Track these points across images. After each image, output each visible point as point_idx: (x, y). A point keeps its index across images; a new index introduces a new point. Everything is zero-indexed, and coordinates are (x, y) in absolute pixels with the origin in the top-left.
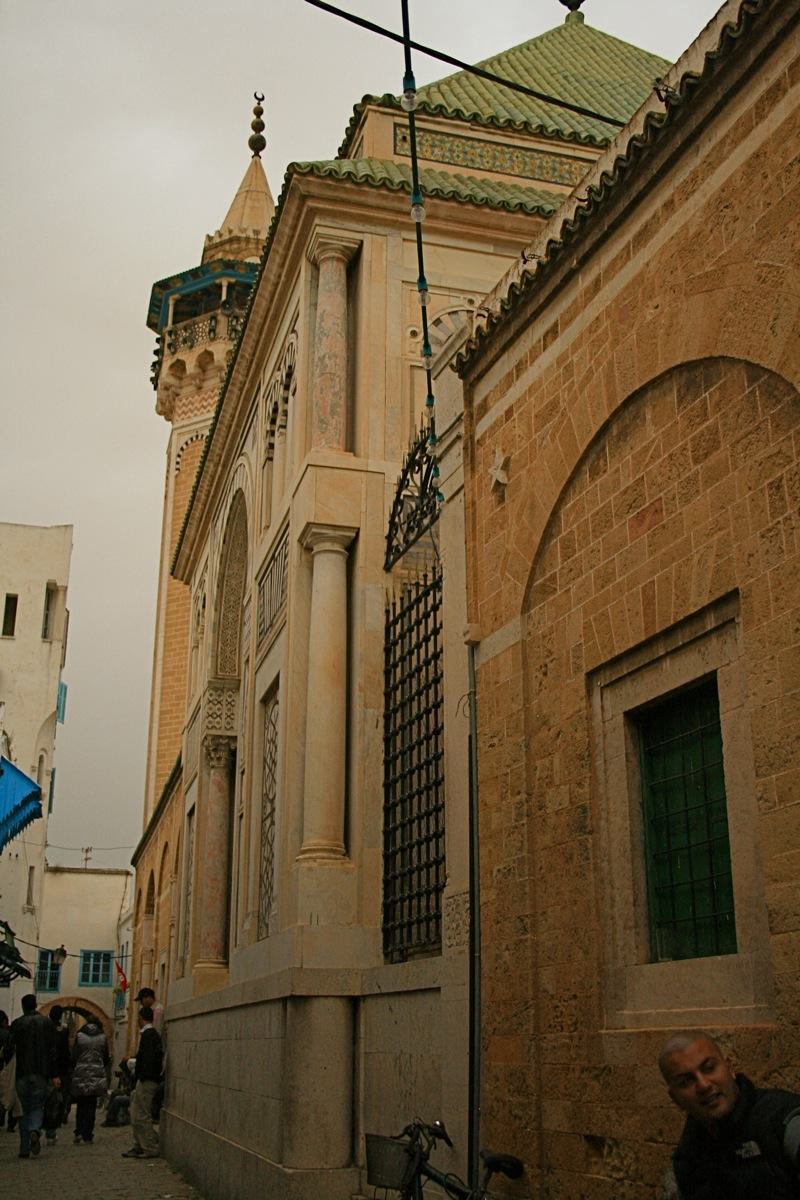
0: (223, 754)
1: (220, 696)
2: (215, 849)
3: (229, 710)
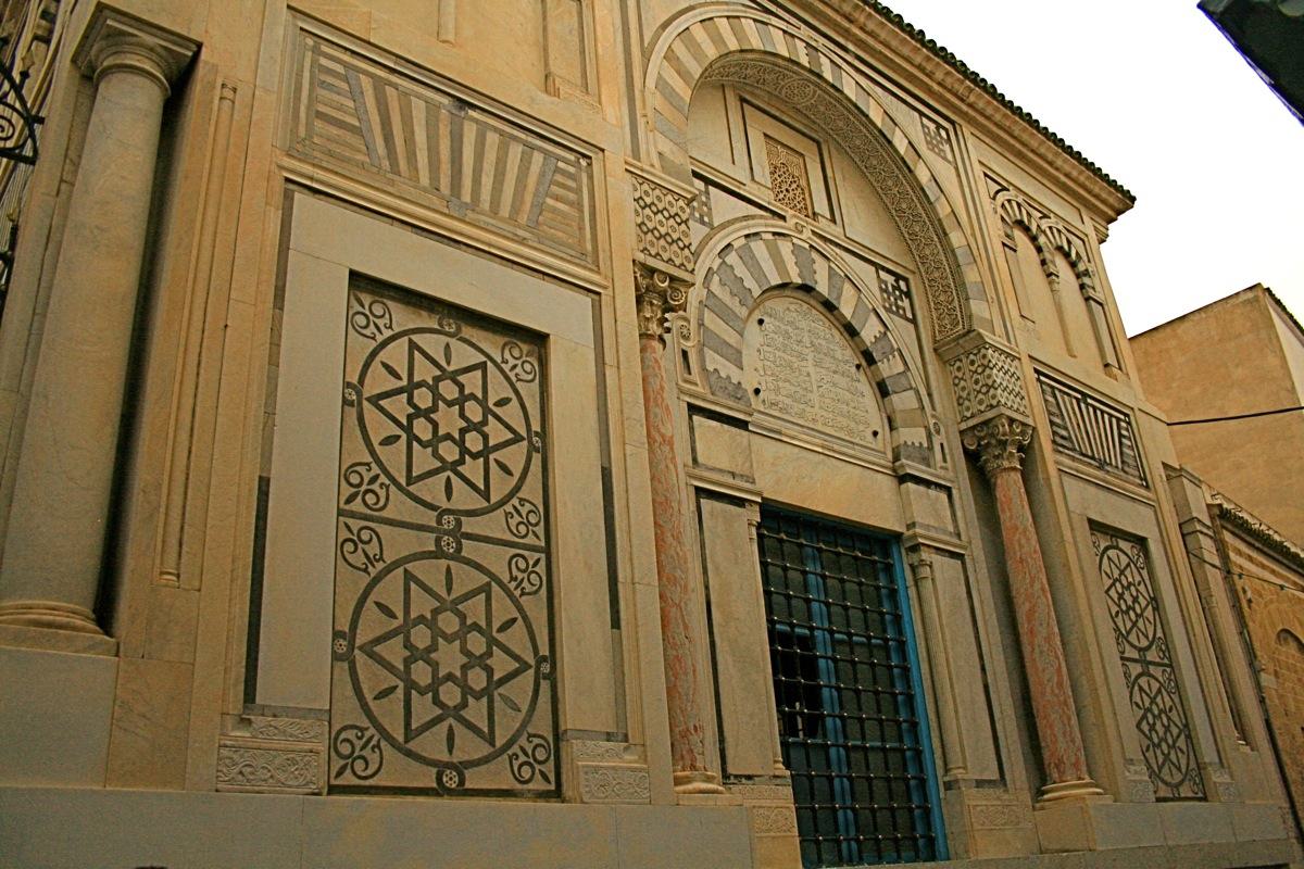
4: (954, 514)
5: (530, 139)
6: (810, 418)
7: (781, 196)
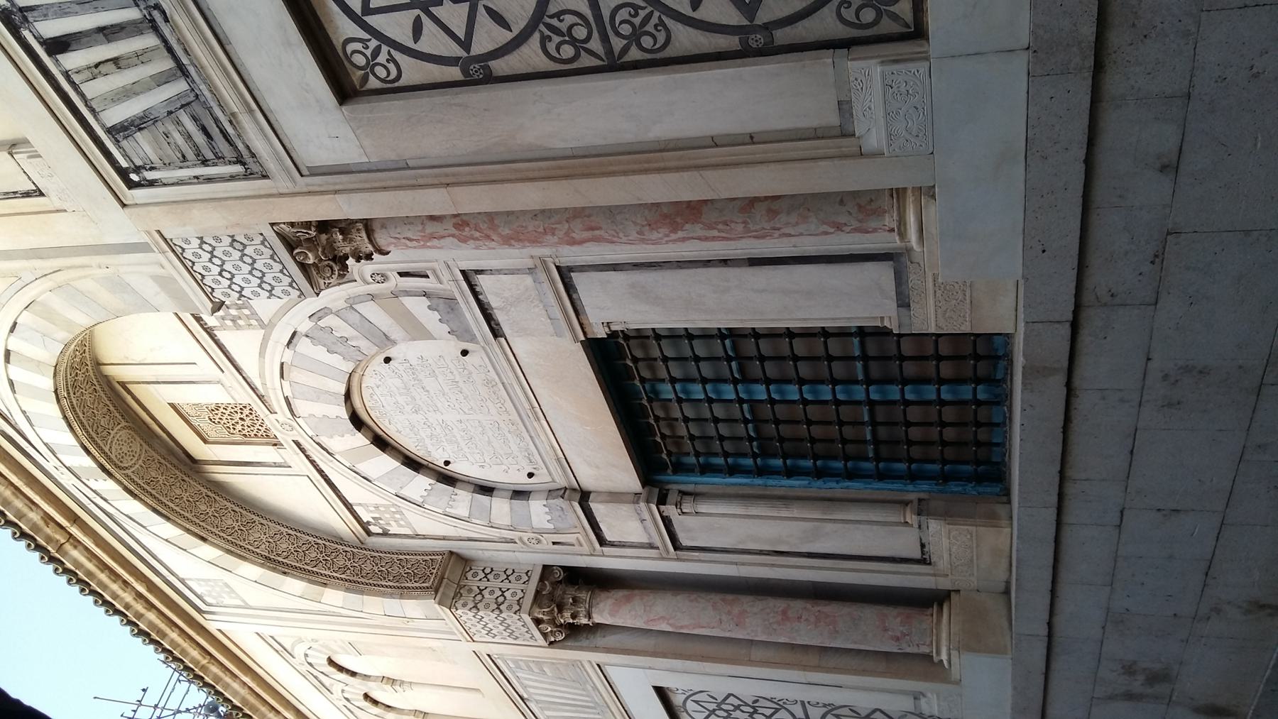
0: (569, 594)
1: (470, 591)
2: (729, 613)
3: (497, 576)
4: (499, 272)
5: (515, 681)
6: (515, 427)
7: (246, 412)
